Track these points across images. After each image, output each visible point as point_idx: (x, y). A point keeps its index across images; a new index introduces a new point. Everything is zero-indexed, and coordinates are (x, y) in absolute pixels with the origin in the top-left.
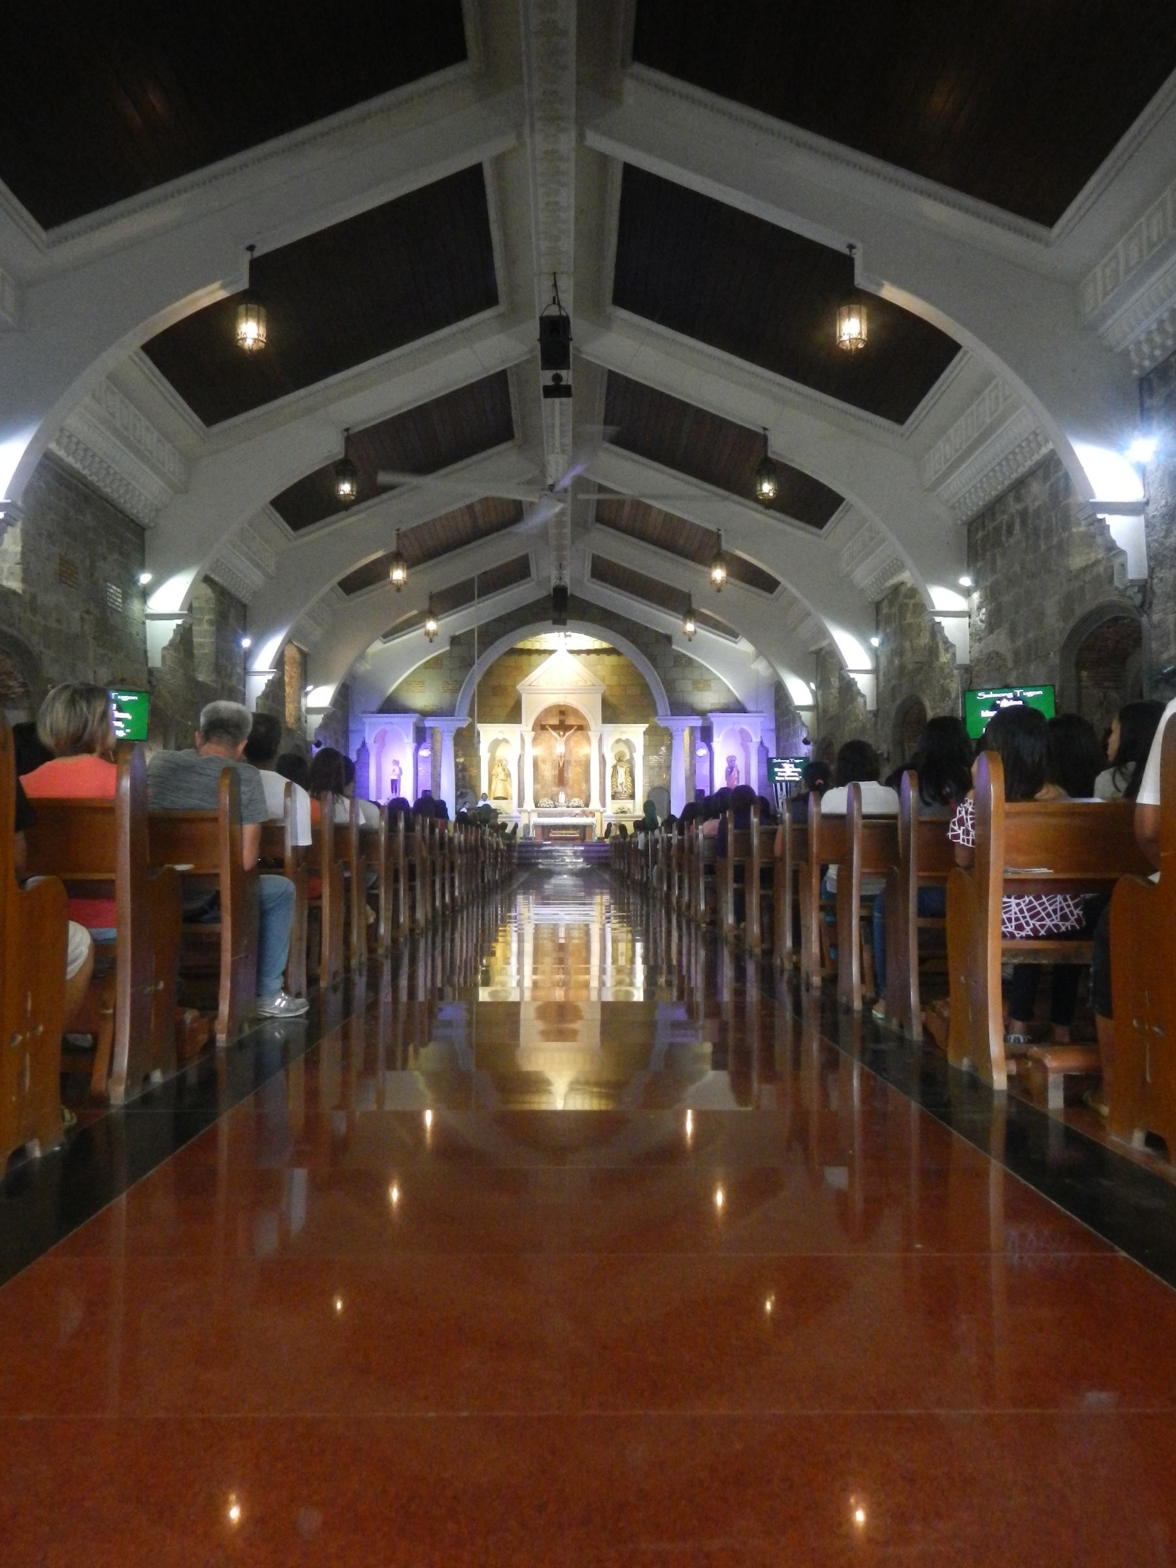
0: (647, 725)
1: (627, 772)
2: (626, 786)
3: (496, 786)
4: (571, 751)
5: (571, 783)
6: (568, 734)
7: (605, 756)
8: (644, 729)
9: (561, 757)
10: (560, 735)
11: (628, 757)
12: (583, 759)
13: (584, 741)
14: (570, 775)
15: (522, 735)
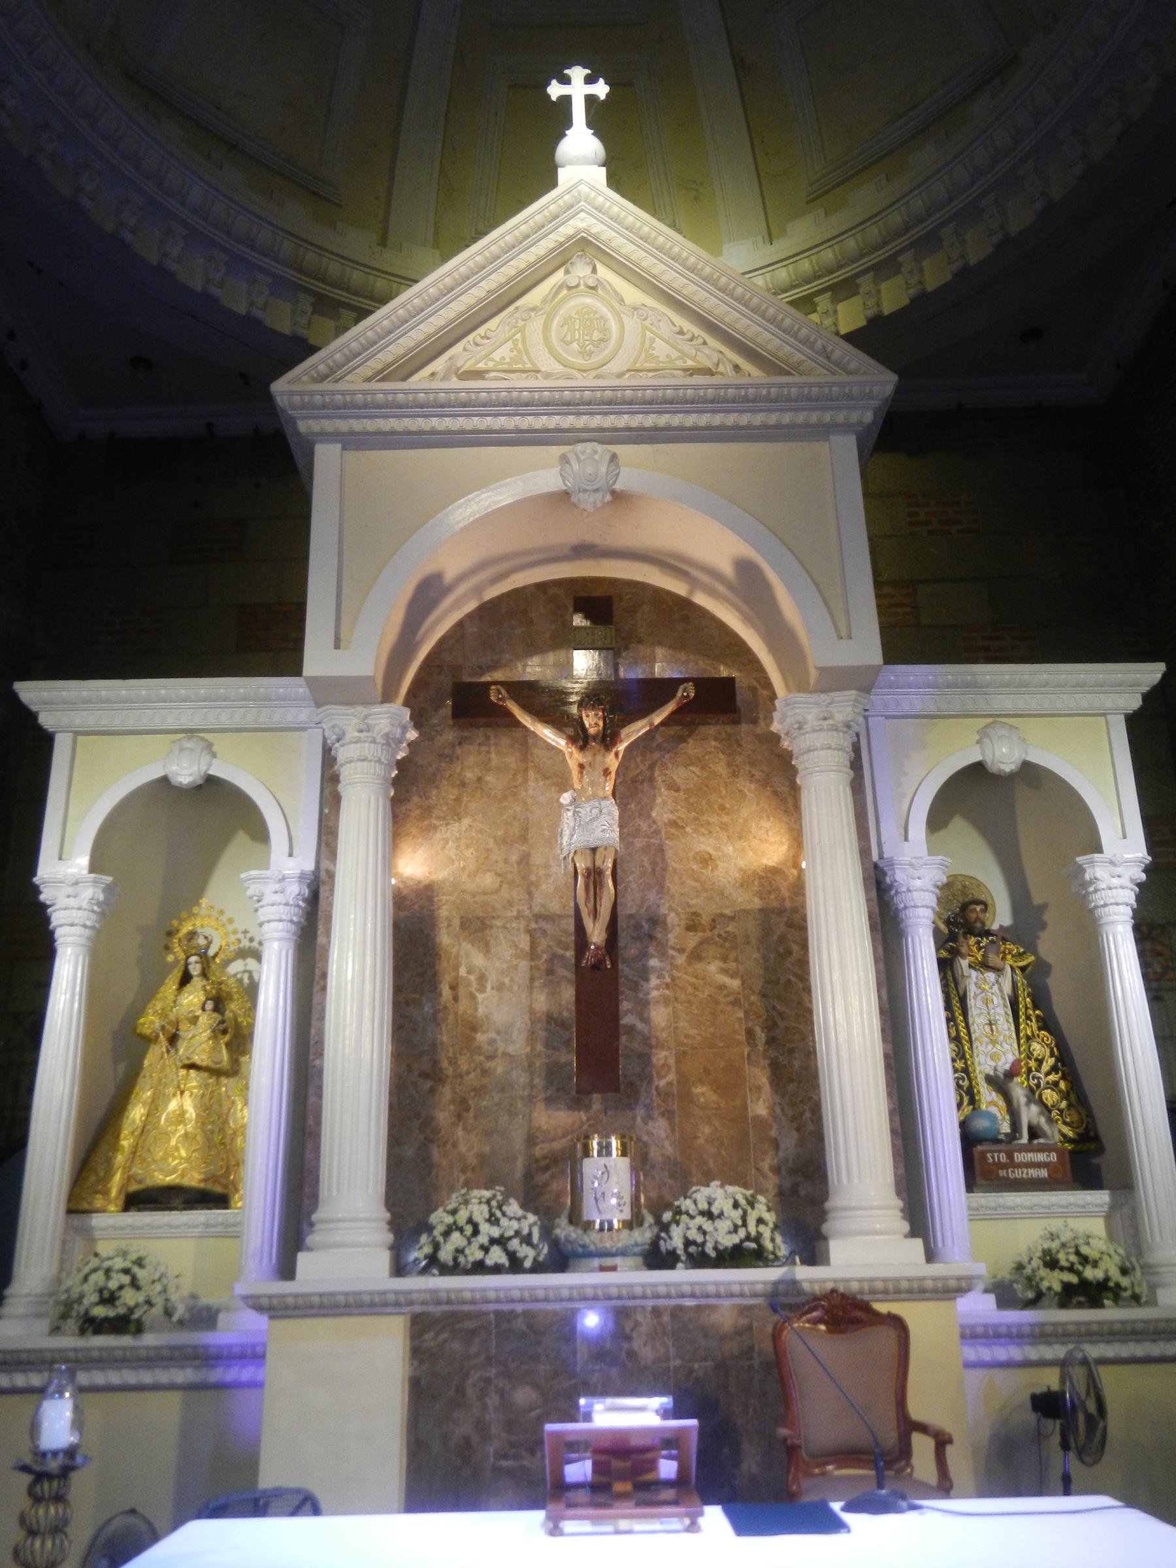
0: (1152, 673)
1: (1025, 1001)
2: (1033, 1094)
3: (154, 1108)
4: (661, 850)
5: (660, 1057)
6: (636, 730)
7: (900, 876)
8: (1135, 703)
9: (594, 876)
10: (581, 738)
11: (1001, 916)
12: (749, 900)
13: (748, 787)
14: (659, 1016)
15: (328, 759)
